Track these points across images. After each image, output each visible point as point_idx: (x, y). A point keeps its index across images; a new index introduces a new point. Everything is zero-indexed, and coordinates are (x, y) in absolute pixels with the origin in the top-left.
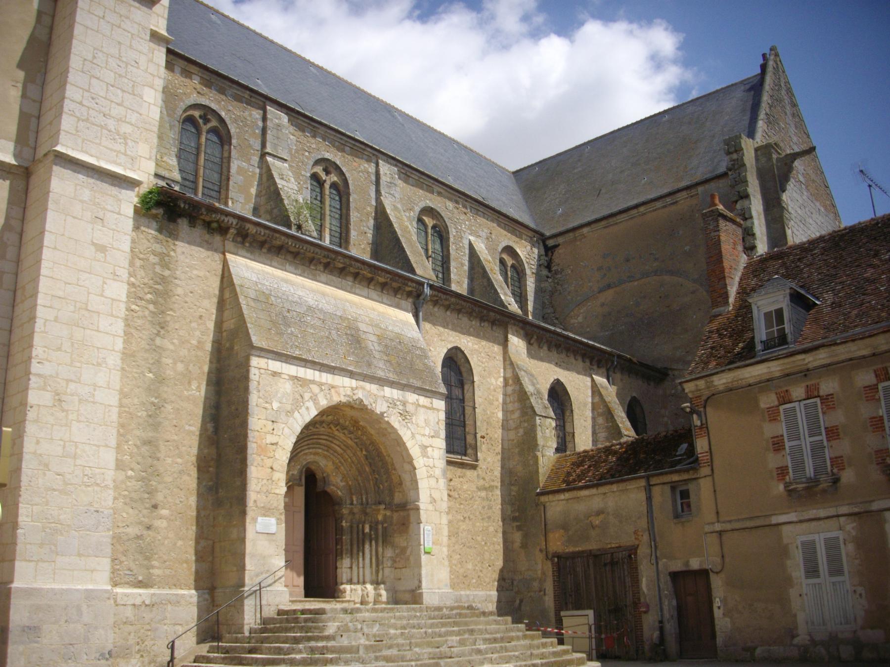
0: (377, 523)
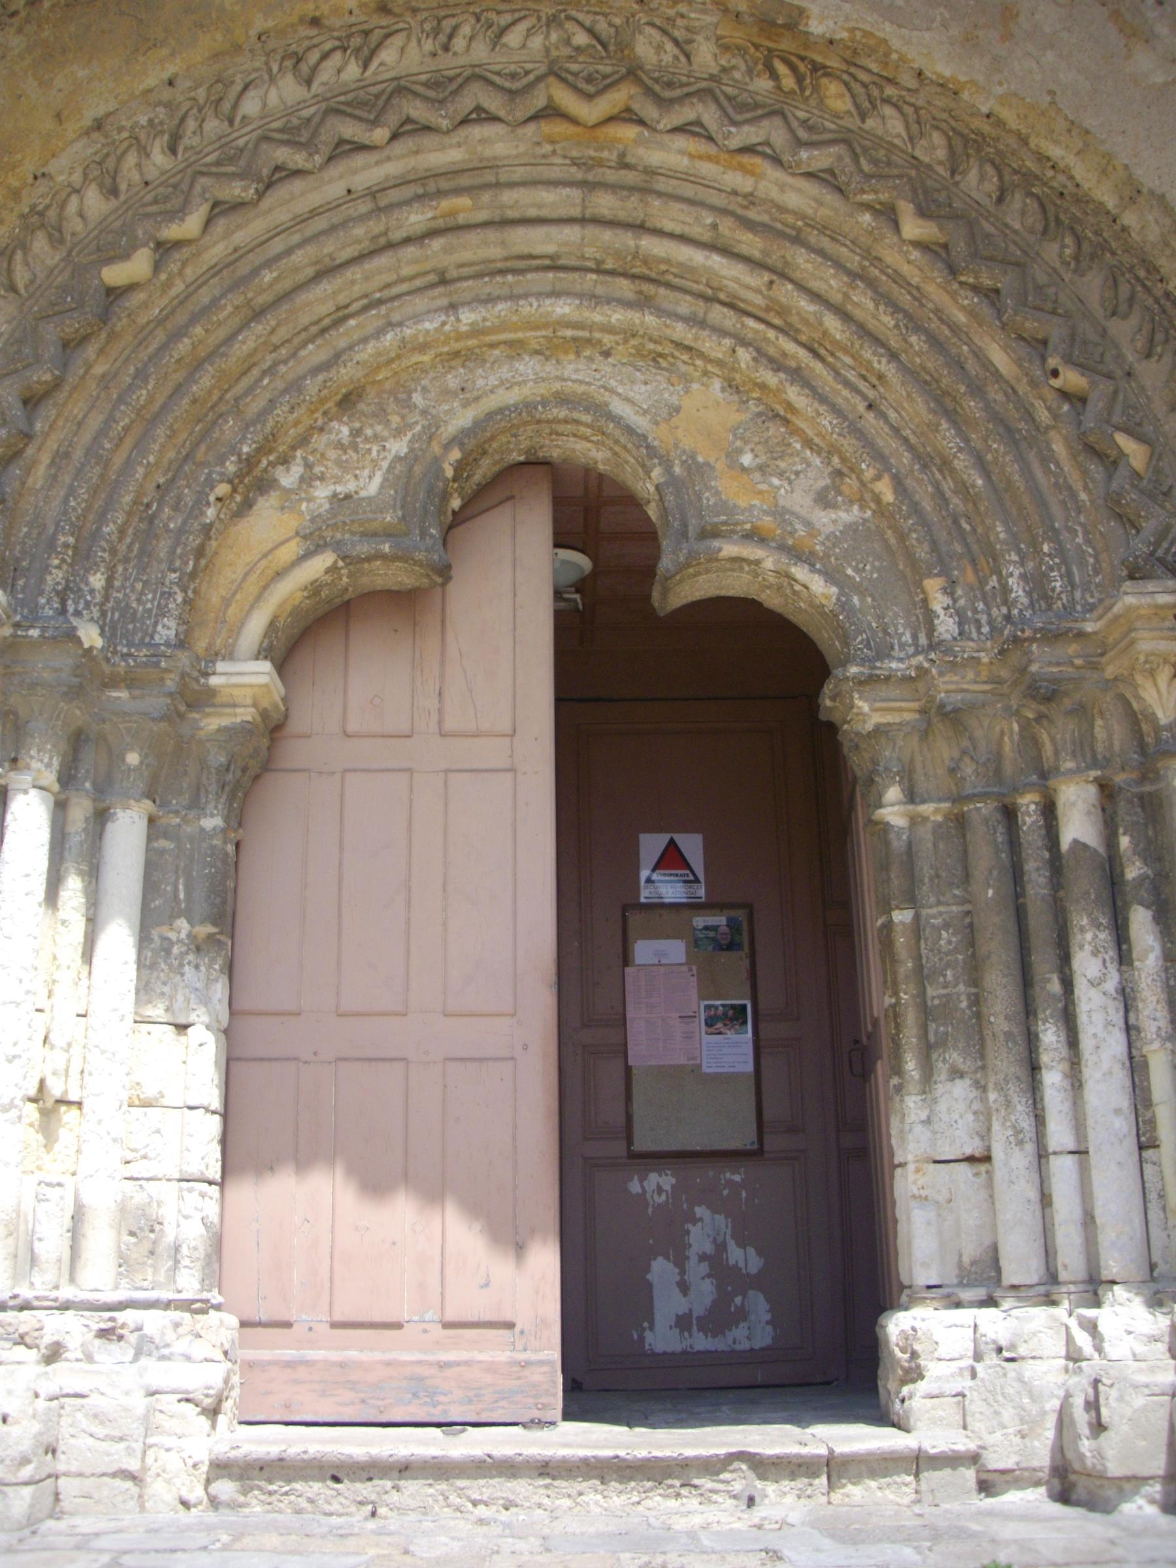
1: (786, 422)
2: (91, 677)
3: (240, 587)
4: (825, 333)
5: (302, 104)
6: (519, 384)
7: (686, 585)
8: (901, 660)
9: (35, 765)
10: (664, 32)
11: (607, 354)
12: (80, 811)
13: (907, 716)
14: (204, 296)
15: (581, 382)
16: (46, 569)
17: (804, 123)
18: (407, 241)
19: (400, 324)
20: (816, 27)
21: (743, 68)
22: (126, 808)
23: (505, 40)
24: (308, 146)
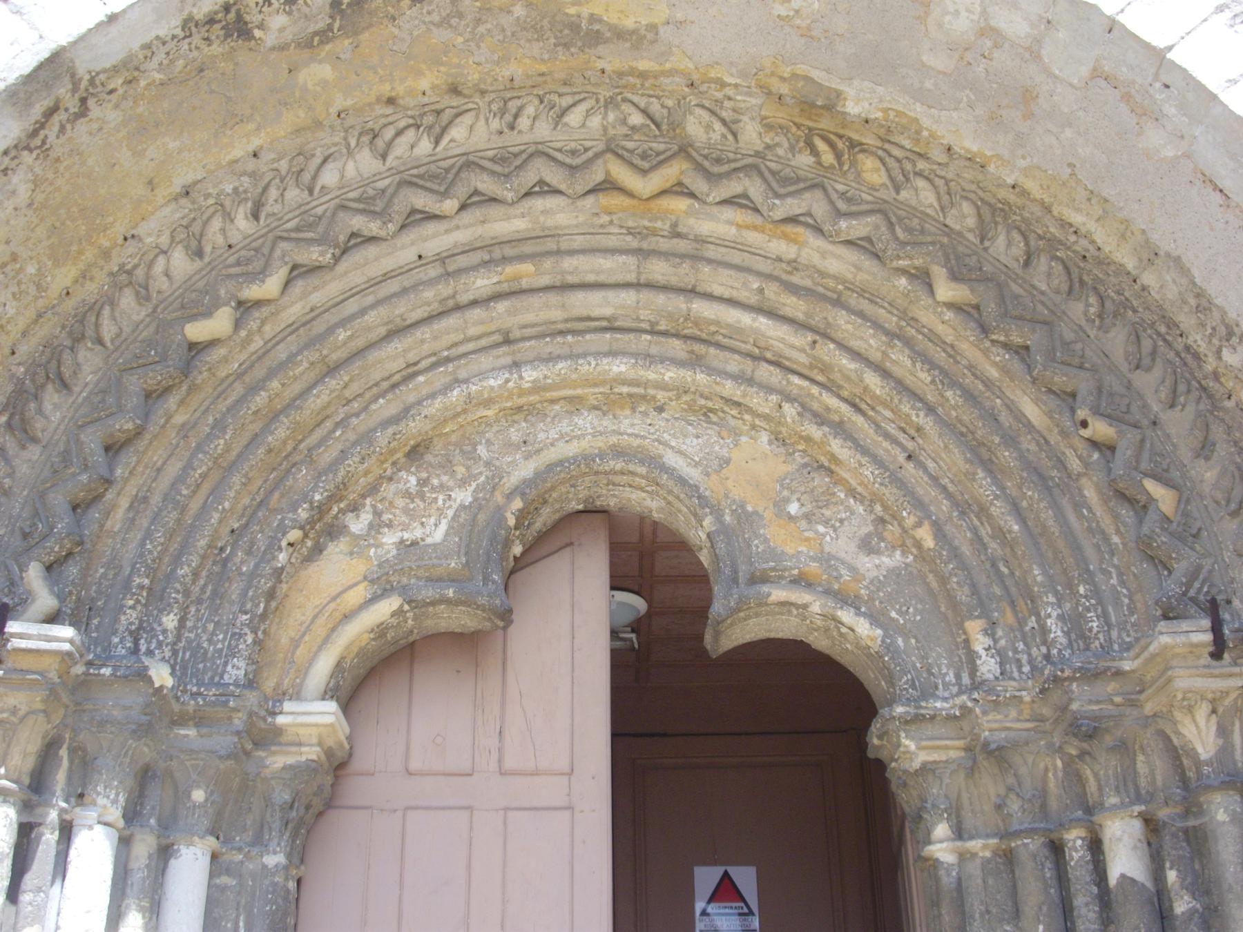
0: (1189, 784)
1: (831, 472)
2: (161, 714)
3: (308, 629)
4: (866, 389)
5: (377, 176)
6: (578, 438)
7: (736, 627)
8: (945, 699)
9: (101, 801)
10: (713, 112)
11: (660, 409)
12: (144, 847)
13: (953, 754)
14: (281, 353)
15: (637, 436)
16: (121, 609)
17: (843, 195)
18: (474, 303)
19: (466, 381)
20: (852, 108)
21: (786, 145)
22: (191, 844)
23: (566, 119)
24: (382, 215)
